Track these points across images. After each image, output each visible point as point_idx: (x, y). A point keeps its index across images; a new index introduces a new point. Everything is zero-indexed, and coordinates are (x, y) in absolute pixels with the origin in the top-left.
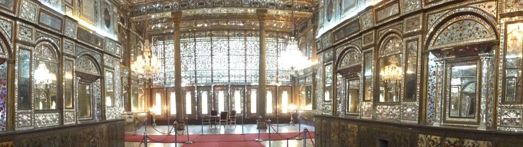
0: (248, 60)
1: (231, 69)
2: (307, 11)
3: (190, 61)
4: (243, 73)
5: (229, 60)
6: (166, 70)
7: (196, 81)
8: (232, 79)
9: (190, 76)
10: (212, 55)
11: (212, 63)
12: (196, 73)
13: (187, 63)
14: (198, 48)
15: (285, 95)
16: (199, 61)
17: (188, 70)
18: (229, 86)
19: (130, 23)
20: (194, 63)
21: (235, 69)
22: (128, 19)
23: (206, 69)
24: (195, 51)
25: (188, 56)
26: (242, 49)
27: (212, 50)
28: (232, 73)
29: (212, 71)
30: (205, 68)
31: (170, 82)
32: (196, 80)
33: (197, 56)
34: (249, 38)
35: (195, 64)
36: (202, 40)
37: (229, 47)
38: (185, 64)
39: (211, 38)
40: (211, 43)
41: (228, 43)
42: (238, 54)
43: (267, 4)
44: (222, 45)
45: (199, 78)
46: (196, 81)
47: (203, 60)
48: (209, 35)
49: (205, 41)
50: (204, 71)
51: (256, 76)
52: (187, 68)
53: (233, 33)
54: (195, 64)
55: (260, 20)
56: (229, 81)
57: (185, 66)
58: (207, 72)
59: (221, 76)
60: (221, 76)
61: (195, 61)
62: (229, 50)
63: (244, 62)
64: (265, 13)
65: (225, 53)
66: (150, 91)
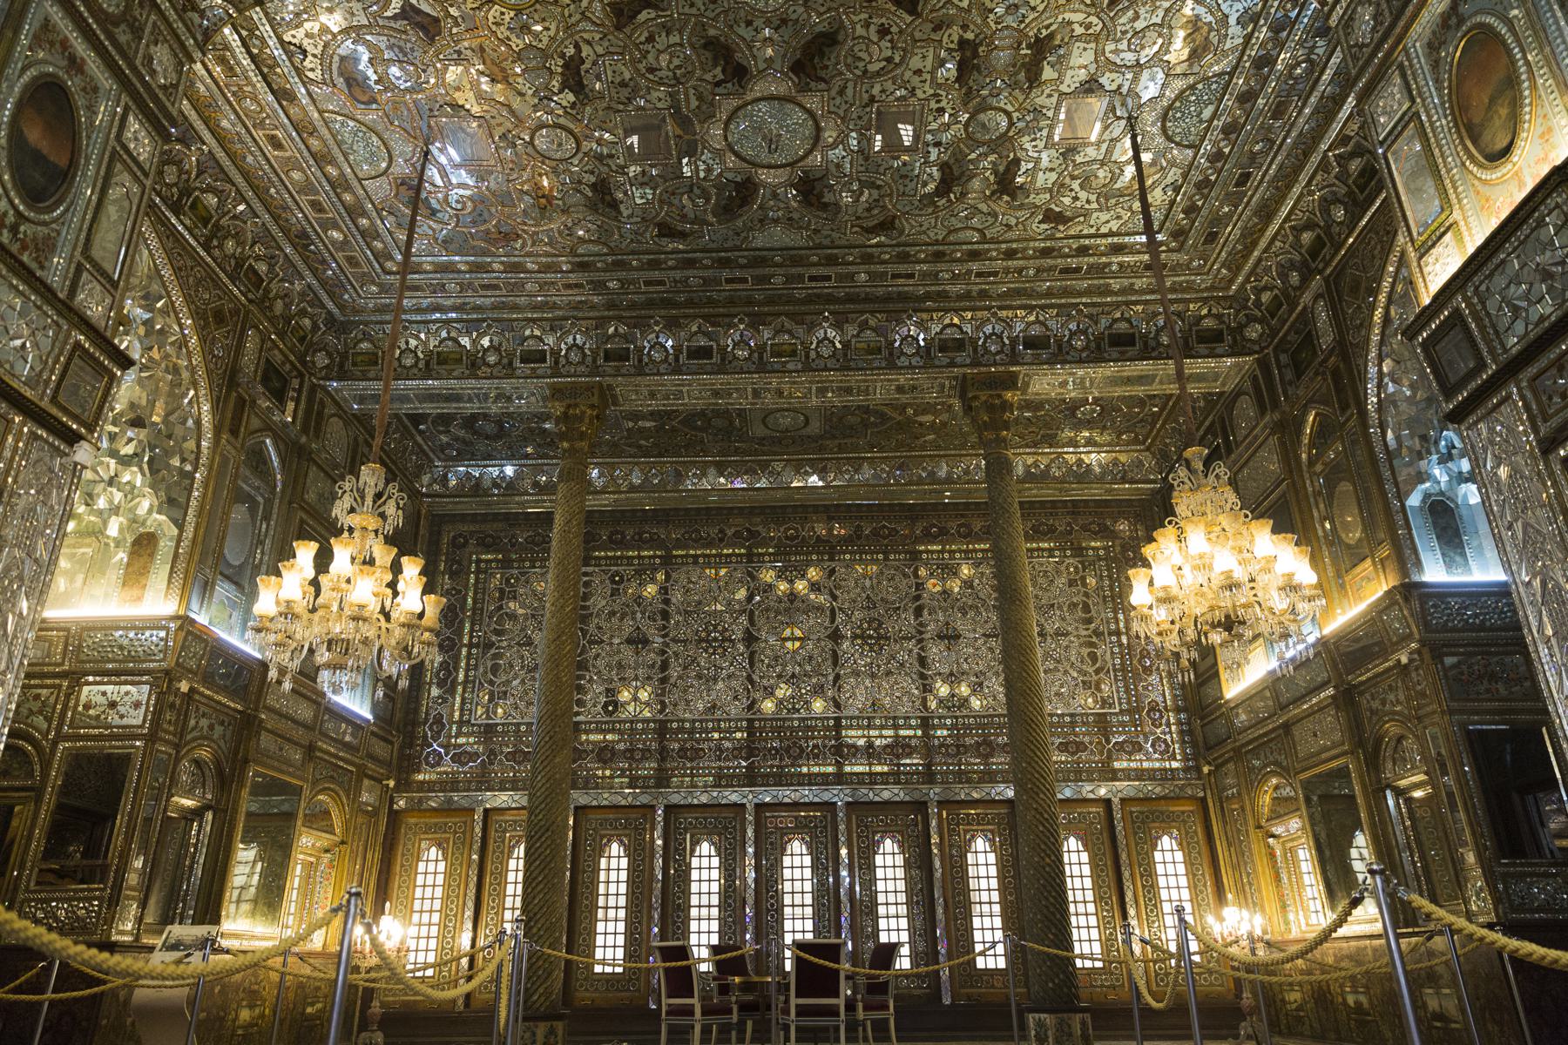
2: (1219, 351)
15: (1169, 858)
19: (320, 414)
22: (313, 389)
32: (659, 770)
43: (1014, 341)
44: (801, 586)
55: (982, 443)
64: (1007, 389)
66: (382, 828)
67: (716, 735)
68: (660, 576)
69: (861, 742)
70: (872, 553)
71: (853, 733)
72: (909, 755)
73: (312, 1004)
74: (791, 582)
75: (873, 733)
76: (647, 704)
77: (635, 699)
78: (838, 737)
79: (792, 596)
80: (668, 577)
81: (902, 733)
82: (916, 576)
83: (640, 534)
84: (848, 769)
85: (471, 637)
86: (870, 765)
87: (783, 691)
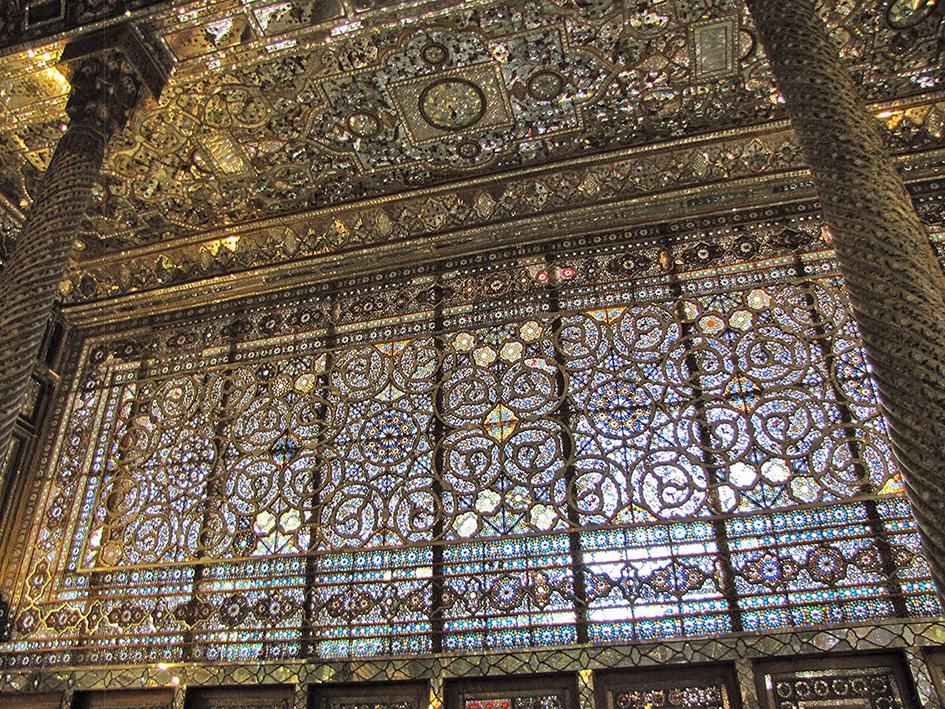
0: (725, 434)
1: (593, 529)
3: (281, 481)
4: (699, 547)
5: (568, 450)
6: (113, 553)
7: (308, 638)
8: (607, 613)
9: (266, 603)
10: (439, 429)
11: (437, 489)
12: (311, 573)
13: (256, 501)
14: (345, 389)
16: (344, 481)
17: (260, 551)
18: (585, 677)
20: (305, 496)
21: (624, 517)
23: (393, 541)
24: (321, 414)
25: (272, 452)
26: (659, 362)
27: (439, 398)
28: (603, 561)
29: (438, 551)
30: (384, 531)
31: (115, 650)
32: (305, 629)
33: (331, 444)
34: (700, 278)
35: (316, 499)
36: (373, 335)
37: (560, 359)
38: (244, 508)
39: (438, 310)
40: (439, 345)
41: (556, 325)
42: (637, 399)
45: (334, 614)
46: (308, 638)
47: (373, 471)
48: (421, 297)
49: (391, 340)
50: (377, 560)
51: (826, 565)
52: (254, 539)
53: (579, 265)
54: (316, 499)
56: (582, 625)
57: (240, 518)
58: (398, 559)
59: (507, 591)
60: (507, 591)
61: (316, 477)
62: (560, 380)
63: (696, 451)
65: (533, 401)
67: (387, 576)
68: (321, 364)
69: (614, 573)
70: (613, 292)
71: (600, 557)
72: (698, 586)
74: (497, 347)
75: (632, 554)
76: (295, 535)
77: (277, 528)
78: (578, 568)
79: (500, 367)
80: (329, 359)
81: (684, 550)
82: (682, 315)
83: (298, 316)
86: (632, 605)
87: (488, 502)
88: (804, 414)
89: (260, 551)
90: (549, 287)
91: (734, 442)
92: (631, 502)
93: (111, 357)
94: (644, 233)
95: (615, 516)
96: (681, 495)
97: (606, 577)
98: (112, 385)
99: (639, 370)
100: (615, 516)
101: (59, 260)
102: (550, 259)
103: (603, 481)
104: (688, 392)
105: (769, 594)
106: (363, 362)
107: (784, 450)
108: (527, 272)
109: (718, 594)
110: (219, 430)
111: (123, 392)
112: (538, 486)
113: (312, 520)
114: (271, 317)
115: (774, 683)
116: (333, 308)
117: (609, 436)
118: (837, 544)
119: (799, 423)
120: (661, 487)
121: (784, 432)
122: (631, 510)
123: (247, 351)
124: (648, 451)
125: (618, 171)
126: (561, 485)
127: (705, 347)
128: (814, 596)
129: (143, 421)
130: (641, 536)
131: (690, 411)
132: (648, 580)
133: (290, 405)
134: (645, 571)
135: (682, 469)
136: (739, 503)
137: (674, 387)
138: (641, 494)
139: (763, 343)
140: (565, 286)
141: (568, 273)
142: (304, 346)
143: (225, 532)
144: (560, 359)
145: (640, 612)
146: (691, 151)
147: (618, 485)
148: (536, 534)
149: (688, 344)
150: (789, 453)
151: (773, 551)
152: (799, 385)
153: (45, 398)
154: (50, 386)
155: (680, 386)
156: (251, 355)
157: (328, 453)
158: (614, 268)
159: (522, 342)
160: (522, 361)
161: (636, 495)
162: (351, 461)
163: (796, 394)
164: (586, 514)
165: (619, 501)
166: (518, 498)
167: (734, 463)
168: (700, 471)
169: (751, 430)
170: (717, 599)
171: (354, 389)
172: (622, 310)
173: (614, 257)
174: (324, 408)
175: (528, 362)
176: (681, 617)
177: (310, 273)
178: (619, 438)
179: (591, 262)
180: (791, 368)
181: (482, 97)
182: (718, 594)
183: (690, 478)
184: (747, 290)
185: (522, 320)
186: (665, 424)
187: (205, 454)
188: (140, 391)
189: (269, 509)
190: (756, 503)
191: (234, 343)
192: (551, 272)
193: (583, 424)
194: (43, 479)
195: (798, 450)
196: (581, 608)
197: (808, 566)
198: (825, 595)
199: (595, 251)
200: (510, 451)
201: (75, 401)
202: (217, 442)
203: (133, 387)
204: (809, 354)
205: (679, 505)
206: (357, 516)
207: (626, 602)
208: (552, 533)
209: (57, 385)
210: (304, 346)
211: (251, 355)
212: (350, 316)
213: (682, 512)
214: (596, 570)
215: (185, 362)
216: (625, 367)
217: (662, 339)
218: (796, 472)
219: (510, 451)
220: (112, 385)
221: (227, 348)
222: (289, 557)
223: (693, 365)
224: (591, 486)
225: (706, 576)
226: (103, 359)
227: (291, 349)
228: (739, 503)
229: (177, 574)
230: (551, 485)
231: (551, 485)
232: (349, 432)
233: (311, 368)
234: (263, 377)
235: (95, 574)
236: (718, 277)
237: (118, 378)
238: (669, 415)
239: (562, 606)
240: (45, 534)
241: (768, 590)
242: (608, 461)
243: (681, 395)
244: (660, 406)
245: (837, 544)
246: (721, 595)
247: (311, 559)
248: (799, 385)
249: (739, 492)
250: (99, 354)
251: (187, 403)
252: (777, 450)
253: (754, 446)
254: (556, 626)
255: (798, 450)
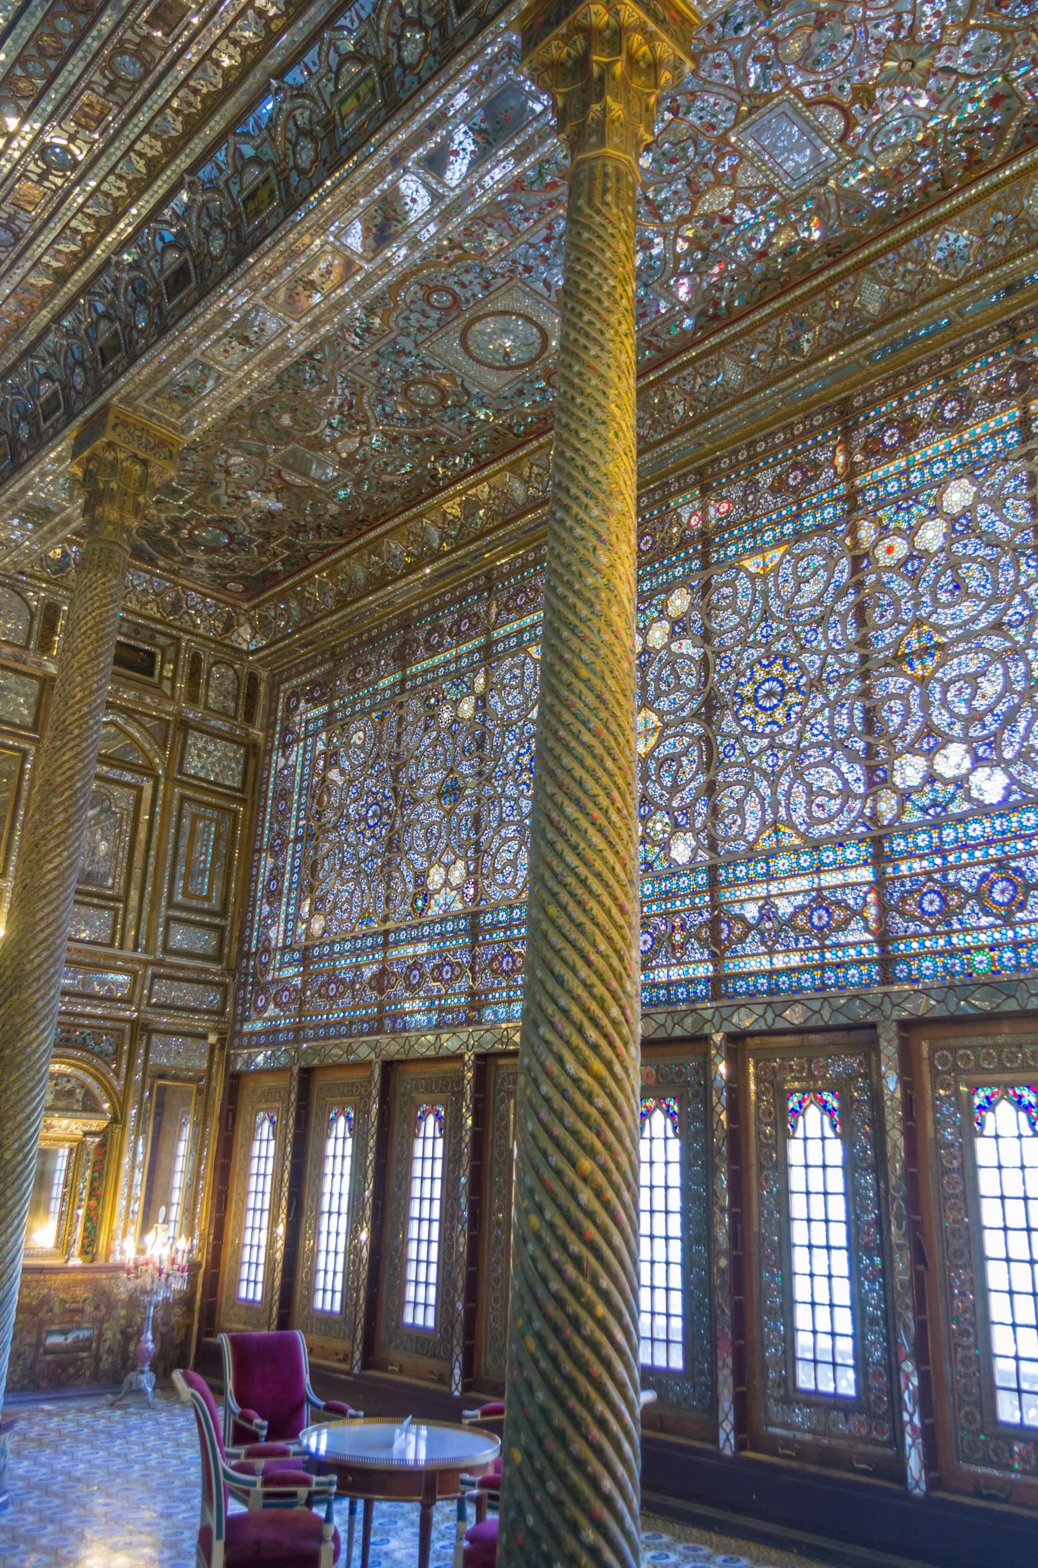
5: (711, 761)
12: (474, 930)
13: (430, 853)
16: (501, 822)
17: (434, 911)
18: (718, 1038)
32: (472, 994)
37: (707, 636)
38: (420, 862)
52: (427, 897)
53: (735, 492)
61: (477, 819)
62: (705, 663)
65: (680, 697)
68: (480, 681)
69: (751, 912)
71: (742, 893)
73: (64, 1332)
75: (774, 888)
76: (459, 888)
81: (830, 879)
84: (731, 967)
85: (297, 828)
86: (771, 952)
88: (1000, 672)
89: (434, 911)
90: (703, 533)
91: (903, 725)
92: (775, 822)
93: (302, 704)
94: (818, 420)
95: (756, 841)
96: (834, 805)
97: (742, 918)
98: (307, 737)
99: (797, 635)
100: (756, 841)
101: (92, 693)
102: (705, 490)
103: (746, 795)
104: (854, 659)
105: (926, 935)
106: (517, 672)
107: (966, 729)
108: (679, 516)
109: (868, 937)
110: (396, 779)
111: (314, 745)
112: (680, 809)
113: (475, 872)
114: (461, 618)
115: (932, 1051)
116: (489, 607)
117: (753, 733)
118: (1020, 863)
119: (990, 687)
120: (810, 792)
121: (968, 702)
122: (776, 831)
123: (415, 676)
124: (799, 751)
125: (763, 341)
126: (701, 808)
127: (881, 586)
128: (982, 937)
129: (334, 775)
130: (782, 863)
131: (855, 685)
132: (790, 922)
133: (454, 735)
134: (785, 907)
135: (837, 770)
136: (902, 810)
137: (836, 653)
138: (787, 807)
139: (955, 567)
140: (719, 529)
141: (723, 508)
142: (464, 662)
143: (404, 893)
144: (707, 636)
145: (779, 962)
146: (851, 279)
147: (762, 799)
148: (674, 871)
149: (859, 585)
150: (972, 733)
151: (937, 876)
152: (997, 627)
153: (252, 762)
154: (255, 746)
155: (842, 650)
156: (419, 681)
157: (488, 791)
158: (779, 487)
159: (669, 618)
160: (667, 647)
161: (782, 812)
162: (507, 799)
163: (994, 642)
164: (726, 839)
165: (763, 820)
166: (659, 827)
167: (900, 754)
168: (859, 771)
169: (926, 705)
170: (865, 943)
171: (509, 709)
172: (783, 549)
173: (778, 469)
174: (483, 734)
175: (674, 647)
176: (822, 967)
177: (459, 568)
178: (762, 735)
179: (753, 486)
180: (994, 598)
181: (528, 320)
182: (868, 937)
183: (845, 782)
184: (942, 485)
185: (668, 589)
186: (821, 710)
187: (385, 804)
188: (330, 740)
189: (440, 862)
190: (924, 810)
191: (403, 669)
192: (704, 509)
193: (728, 724)
194: (259, 851)
195: (984, 726)
196: (716, 958)
197: (977, 895)
198: (997, 936)
199: (756, 465)
200: (653, 765)
201: (278, 760)
202: (394, 789)
203: (324, 736)
204: (1018, 574)
205: (830, 819)
206: (513, 863)
207: (762, 949)
208: (692, 867)
209: (261, 742)
210: (464, 662)
211: (419, 681)
212: (504, 615)
213: (832, 828)
214: (736, 909)
215: (363, 699)
216: (779, 636)
217: (828, 583)
218: (978, 761)
219: (653, 765)
220: (307, 737)
221: (398, 676)
222: (456, 917)
223: (860, 612)
224: (732, 803)
225: (855, 913)
226: (297, 707)
227: (452, 667)
228: (902, 810)
229: (369, 942)
230: (693, 804)
231: (693, 804)
232: (506, 764)
233: (471, 687)
234: (429, 706)
235: (307, 948)
236: (906, 472)
237: (311, 727)
238: (826, 697)
239: (698, 956)
240: (266, 909)
241: (926, 929)
242: (752, 768)
243: (845, 665)
244: (816, 685)
245: (1020, 863)
246: (870, 938)
247: (474, 916)
248: (997, 627)
249: (905, 796)
250: (293, 702)
251: (368, 747)
252: (957, 730)
253: (929, 729)
254: (751, 974)
255: (984, 726)
